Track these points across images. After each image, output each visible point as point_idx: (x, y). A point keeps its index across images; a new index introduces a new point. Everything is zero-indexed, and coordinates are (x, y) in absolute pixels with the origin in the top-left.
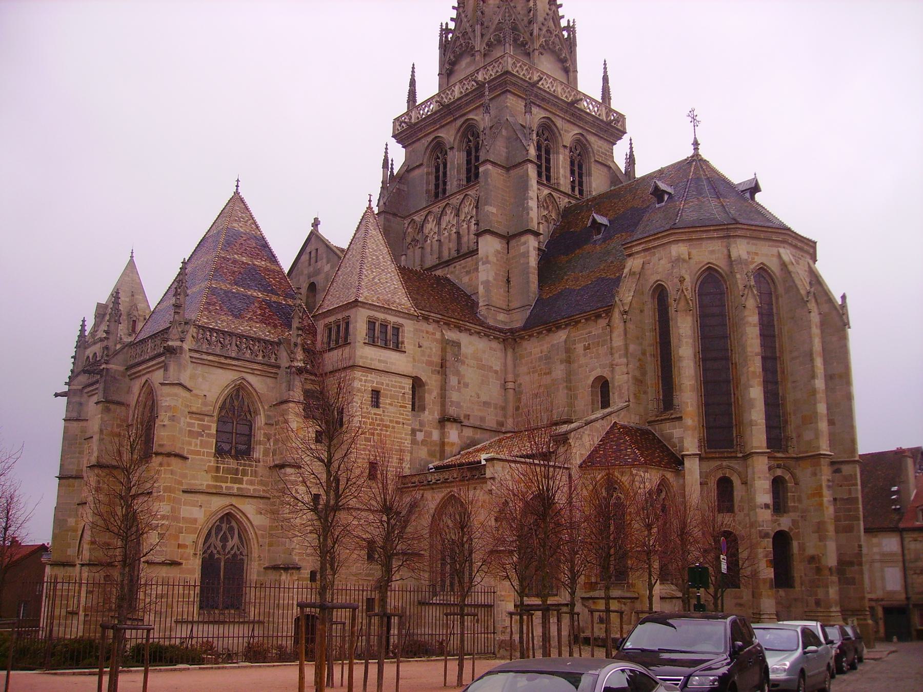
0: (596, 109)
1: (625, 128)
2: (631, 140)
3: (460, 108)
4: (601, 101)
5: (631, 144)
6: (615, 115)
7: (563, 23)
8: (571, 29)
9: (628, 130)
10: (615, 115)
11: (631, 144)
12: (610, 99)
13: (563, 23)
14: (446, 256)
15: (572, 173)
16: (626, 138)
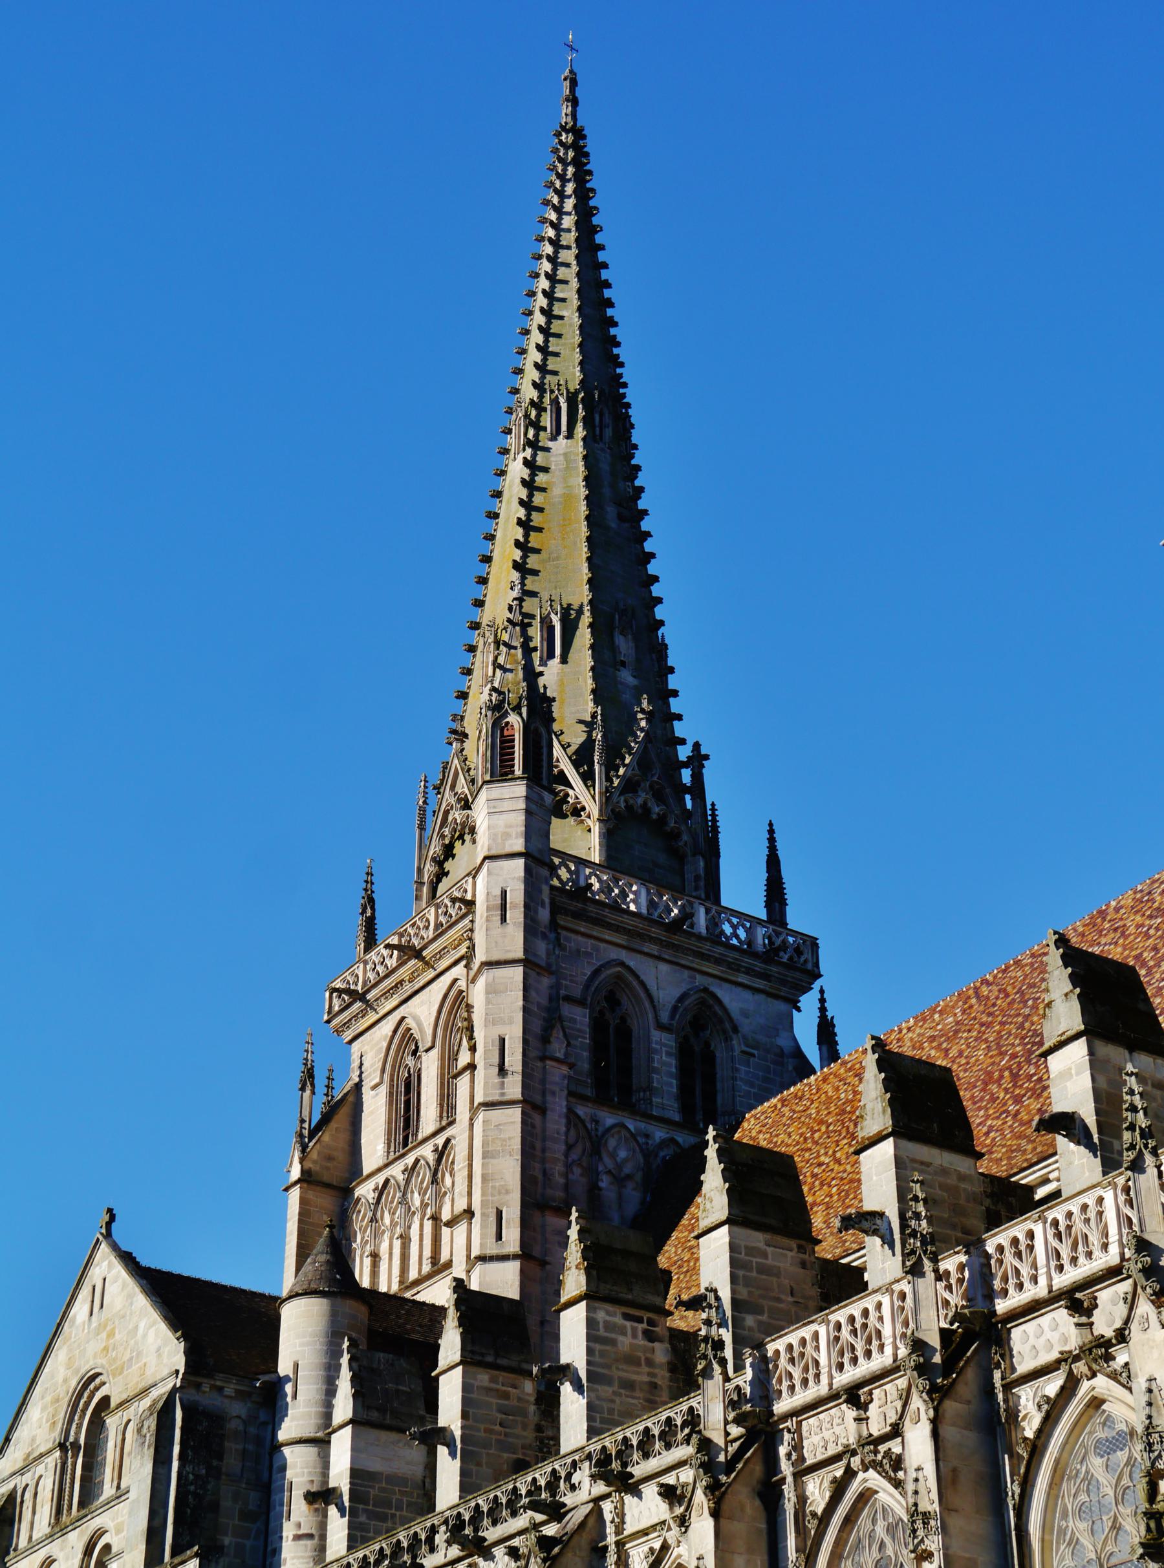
0: (742, 933)
1: (817, 964)
2: (822, 992)
3: (440, 955)
4: (762, 914)
5: (822, 1001)
6: (791, 939)
7: (684, 752)
8: (698, 759)
9: (823, 969)
10: (791, 939)
11: (822, 1001)
12: (783, 903)
13: (684, 752)
14: (413, 1275)
15: (685, 1073)
16: (816, 986)
